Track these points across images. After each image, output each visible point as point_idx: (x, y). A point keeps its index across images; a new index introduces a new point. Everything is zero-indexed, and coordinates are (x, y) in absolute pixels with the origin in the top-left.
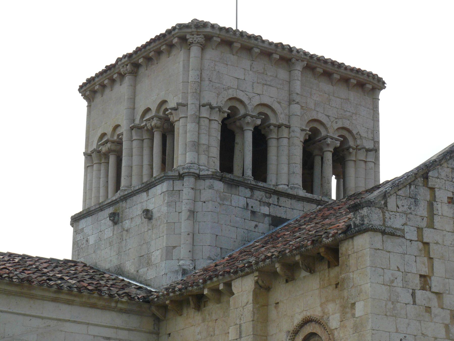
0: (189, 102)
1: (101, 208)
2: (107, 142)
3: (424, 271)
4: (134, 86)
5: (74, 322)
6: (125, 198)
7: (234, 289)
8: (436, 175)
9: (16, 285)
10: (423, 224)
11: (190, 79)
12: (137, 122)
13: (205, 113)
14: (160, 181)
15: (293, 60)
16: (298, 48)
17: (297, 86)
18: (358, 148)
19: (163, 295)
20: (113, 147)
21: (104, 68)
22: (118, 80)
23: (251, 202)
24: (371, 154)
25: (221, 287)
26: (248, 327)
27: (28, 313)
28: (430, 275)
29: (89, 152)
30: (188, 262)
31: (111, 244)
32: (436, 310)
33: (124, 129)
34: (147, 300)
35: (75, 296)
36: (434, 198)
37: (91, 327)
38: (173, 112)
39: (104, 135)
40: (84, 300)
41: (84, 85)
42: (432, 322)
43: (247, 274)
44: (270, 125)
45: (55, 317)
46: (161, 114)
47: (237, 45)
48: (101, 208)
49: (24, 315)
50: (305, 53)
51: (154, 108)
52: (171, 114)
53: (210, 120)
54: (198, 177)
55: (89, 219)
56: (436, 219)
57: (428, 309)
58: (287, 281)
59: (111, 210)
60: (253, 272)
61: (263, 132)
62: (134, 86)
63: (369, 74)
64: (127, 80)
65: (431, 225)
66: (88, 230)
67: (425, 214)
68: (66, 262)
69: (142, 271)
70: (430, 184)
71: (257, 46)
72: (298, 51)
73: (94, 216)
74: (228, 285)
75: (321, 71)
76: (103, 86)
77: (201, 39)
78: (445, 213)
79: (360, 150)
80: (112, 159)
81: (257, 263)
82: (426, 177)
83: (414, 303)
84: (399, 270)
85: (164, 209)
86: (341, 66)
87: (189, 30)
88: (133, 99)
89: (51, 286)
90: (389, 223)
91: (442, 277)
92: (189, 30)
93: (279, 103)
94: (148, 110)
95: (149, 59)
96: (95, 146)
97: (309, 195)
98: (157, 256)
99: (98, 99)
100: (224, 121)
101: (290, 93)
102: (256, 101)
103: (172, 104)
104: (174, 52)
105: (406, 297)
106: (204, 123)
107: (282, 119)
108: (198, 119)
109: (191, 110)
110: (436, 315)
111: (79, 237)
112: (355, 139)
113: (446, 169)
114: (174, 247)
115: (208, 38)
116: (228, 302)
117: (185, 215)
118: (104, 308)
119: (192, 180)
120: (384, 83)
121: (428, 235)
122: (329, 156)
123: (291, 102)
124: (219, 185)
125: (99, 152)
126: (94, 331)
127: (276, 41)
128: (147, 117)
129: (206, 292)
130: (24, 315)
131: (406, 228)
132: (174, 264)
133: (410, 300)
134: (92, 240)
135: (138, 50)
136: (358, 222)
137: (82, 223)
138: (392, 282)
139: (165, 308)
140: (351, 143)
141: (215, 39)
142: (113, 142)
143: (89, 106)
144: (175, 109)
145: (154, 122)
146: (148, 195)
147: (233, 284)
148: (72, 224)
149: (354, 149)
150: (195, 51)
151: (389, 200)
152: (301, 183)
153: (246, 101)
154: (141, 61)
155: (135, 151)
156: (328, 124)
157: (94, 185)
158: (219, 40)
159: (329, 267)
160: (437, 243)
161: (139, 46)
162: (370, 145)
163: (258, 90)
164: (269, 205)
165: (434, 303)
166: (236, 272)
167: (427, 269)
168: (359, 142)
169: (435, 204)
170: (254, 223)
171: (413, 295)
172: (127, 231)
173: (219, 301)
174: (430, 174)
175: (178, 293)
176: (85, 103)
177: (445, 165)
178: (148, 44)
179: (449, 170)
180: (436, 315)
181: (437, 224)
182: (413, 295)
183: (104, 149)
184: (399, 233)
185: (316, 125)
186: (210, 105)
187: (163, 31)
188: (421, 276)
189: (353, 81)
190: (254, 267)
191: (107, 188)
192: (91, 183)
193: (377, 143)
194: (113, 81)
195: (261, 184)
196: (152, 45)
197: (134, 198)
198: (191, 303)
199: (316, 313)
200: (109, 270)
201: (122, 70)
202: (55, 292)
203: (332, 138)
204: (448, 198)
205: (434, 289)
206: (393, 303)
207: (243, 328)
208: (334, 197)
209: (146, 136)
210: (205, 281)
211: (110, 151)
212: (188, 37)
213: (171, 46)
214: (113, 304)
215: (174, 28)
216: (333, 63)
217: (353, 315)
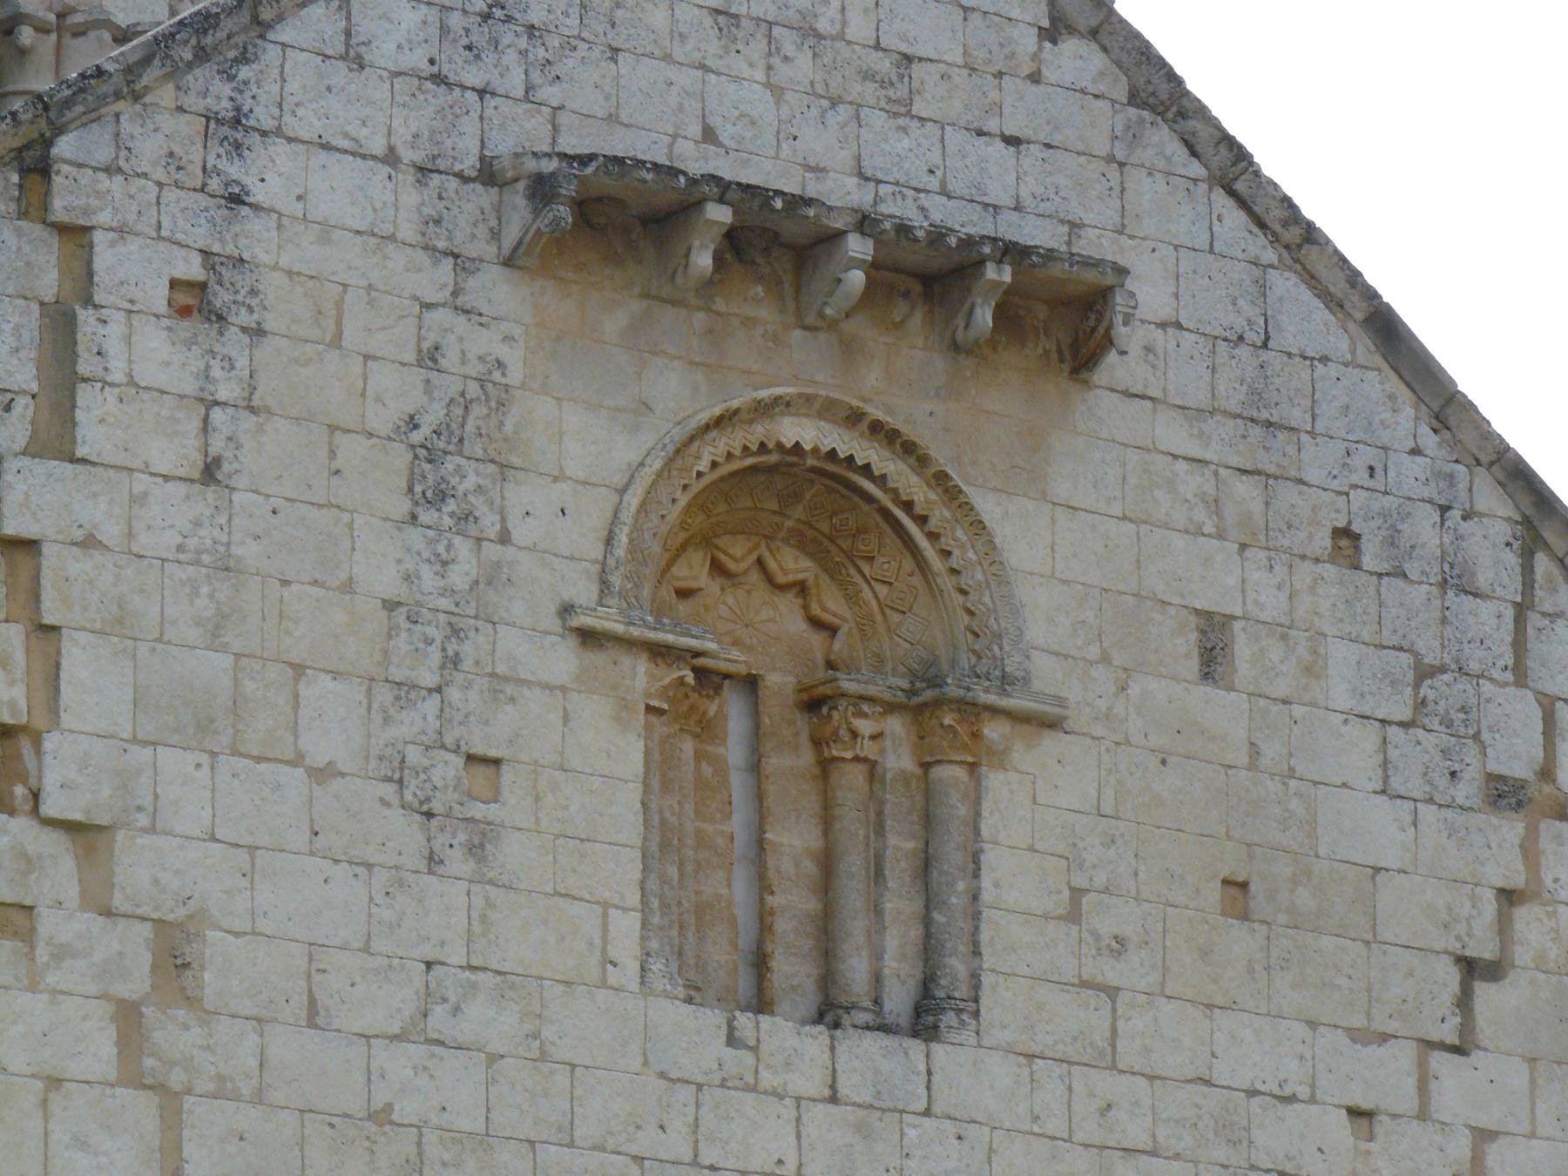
8: (104, 154)
28: (39, 723)
36: (83, 284)
42: (33, 988)
56: (91, 406)
70: (62, 205)
78: (148, 373)
79: (79, 33)
91: (113, 737)
110: (62, 953)
113: (167, 121)
149: (42, 29)
160: (89, 543)
167: (19, 693)
169: (85, 316)
174: (64, 146)
177: (166, 95)
179: (189, 126)
180: (62, 953)
181: (91, 436)
204: (174, 284)
205: (50, 808)
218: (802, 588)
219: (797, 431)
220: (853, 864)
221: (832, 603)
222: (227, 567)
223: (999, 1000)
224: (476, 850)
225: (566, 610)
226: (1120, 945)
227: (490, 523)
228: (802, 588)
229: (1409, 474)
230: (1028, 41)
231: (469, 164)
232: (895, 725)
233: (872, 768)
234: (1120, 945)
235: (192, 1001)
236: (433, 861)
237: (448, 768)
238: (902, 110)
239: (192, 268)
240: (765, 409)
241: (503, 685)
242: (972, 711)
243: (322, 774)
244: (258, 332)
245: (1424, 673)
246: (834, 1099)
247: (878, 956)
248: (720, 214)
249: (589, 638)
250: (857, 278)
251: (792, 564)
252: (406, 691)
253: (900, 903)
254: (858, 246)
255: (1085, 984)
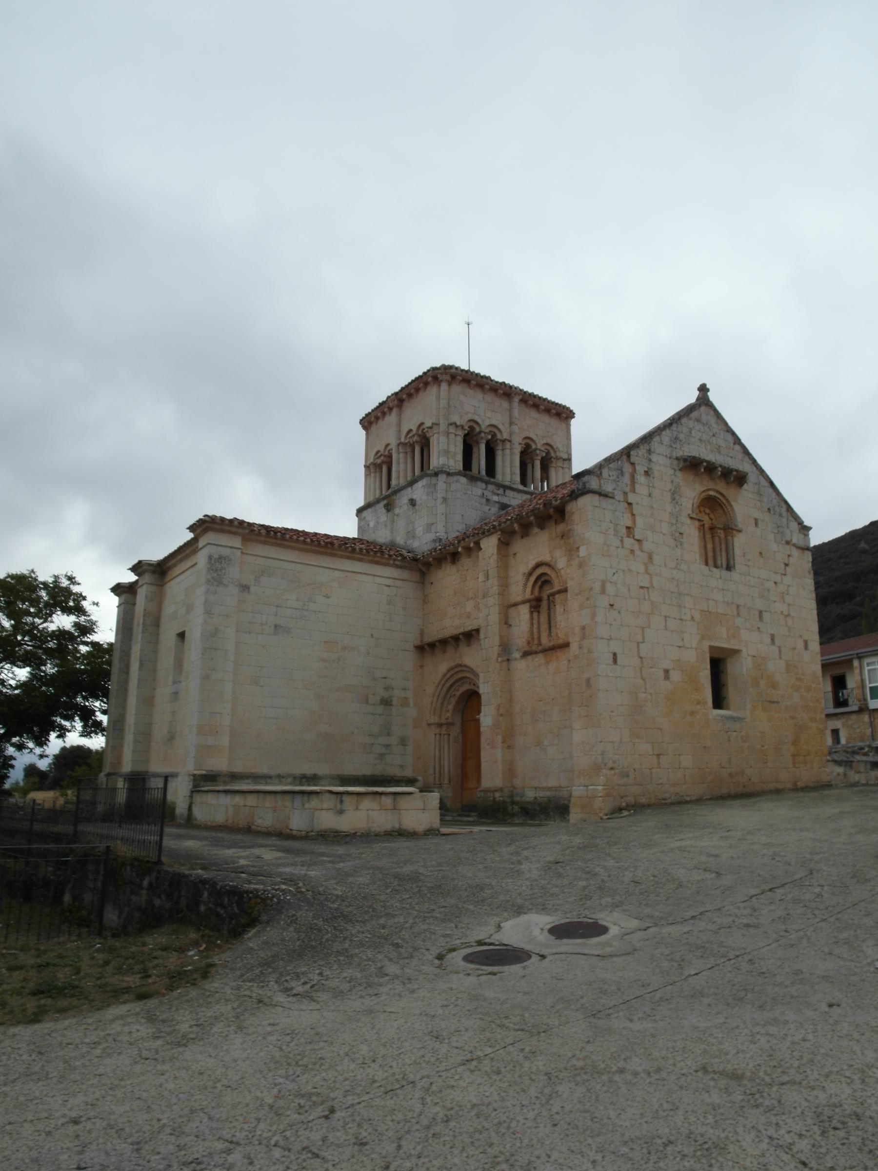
0: (441, 422)
1: (378, 501)
2: (380, 456)
3: (629, 524)
4: (400, 415)
5: (365, 574)
6: (395, 493)
7: (482, 546)
9: (322, 547)
10: (628, 490)
11: (441, 406)
12: (403, 440)
13: (452, 429)
14: (421, 478)
15: (513, 395)
16: (516, 386)
17: (516, 412)
18: (558, 458)
19: (427, 555)
20: (386, 459)
21: (378, 405)
22: (388, 413)
23: (486, 493)
24: (566, 462)
25: (472, 545)
26: (493, 572)
27: (331, 567)
29: (368, 464)
30: (443, 534)
31: (385, 525)
32: (638, 553)
33: (393, 445)
34: (415, 560)
35: (364, 555)
36: (634, 470)
37: (376, 578)
38: (429, 430)
39: (378, 452)
40: (370, 558)
41: (364, 418)
43: (492, 534)
44: (497, 439)
45: (351, 570)
46: (420, 432)
47: (474, 382)
48: (378, 501)
49: (329, 568)
50: (521, 390)
51: (414, 429)
52: (427, 431)
53: (456, 435)
54: (448, 474)
55: (369, 510)
56: (637, 486)
57: (632, 551)
58: (522, 537)
59: (385, 502)
60: (496, 532)
61: (492, 445)
62: (400, 415)
63: (564, 407)
64: (395, 411)
65: (633, 490)
66: (369, 518)
67: (629, 482)
68: (354, 539)
69: (409, 542)
70: (632, 460)
71: (488, 384)
72: (516, 388)
73: (373, 508)
74: (477, 544)
75: (532, 403)
76: (377, 418)
77: (448, 377)
78: (642, 482)
80: (385, 468)
81: (500, 525)
82: (629, 456)
83: (623, 547)
84: (611, 522)
85: (425, 497)
86: (545, 400)
87: (440, 371)
88: (399, 424)
89: (347, 548)
90: (604, 488)
92: (440, 371)
93: (503, 424)
94: (410, 431)
95: (410, 395)
96: (372, 460)
97: (525, 489)
98: (419, 531)
99: (374, 428)
100: (465, 436)
101: (511, 417)
102: (487, 423)
103: (428, 424)
104: (429, 388)
105: (616, 542)
106: (452, 436)
107: (506, 436)
108: (448, 434)
109: (443, 427)
111: (362, 523)
112: (555, 452)
114: (432, 524)
115: (453, 377)
116: (478, 557)
117: (440, 500)
118: (385, 565)
119: (444, 476)
120: (574, 414)
121: (631, 498)
122: (538, 464)
123: (511, 424)
124: (463, 480)
125: (375, 464)
126: (378, 580)
127: (501, 381)
128: (410, 435)
129: (460, 549)
130: (329, 568)
131: (616, 493)
132: (431, 536)
133: (619, 544)
134: (372, 524)
135: (403, 389)
136: (580, 487)
137: (365, 514)
138: (607, 531)
139: (428, 565)
140: (553, 454)
141: (458, 377)
142: (385, 456)
143: (367, 434)
144: (430, 428)
145: (416, 438)
146: (412, 489)
147: (481, 542)
148: (357, 515)
150: (444, 386)
151: (603, 471)
152: (519, 480)
153: (481, 423)
154: (404, 397)
155: (401, 460)
156: (537, 441)
157: (372, 487)
158: (461, 378)
159: (556, 524)
160: (638, 504)
161: (403, 386)
162: (565, 456)
163: (489, 414)
164: (498, 495)
165: (636, 547)
166: (483, 533)
168: (558, 454)
170: (488, 508)
171: (622, 541)
172: (397, 515)
173: (469, 556)
174: (632, 453)
175: (438, 552)
176: (363, 433)
178: (410, 384)
181: (637, 490)
182: (622, 541)
183: (379, 461)
184: (610, 495)
185: (528, 441)
186: (455, 424)
187: (421, 374)
188: (628, 528)
189: (554, 411)
190: (498, 528)
191: (381, 485)
192: (370, 486)
193: (570, 455)
194: (384, 414)
195: (492, 480)
196: (413, 385)
197: (402, 492)
198: (449, 558)
199: (547, 558)
200: (384, 544)
201: (391, 405)
202: (351, 552)
203: (540, 450)
206: (608, 546)
207: (490, 572)
208: (546, 489)
209: (409, 449)
210: (459, 542)
211: (383, 462)
212: (439, 376)
213: (426, 384)
214: (391, 562)
215: (429, 371)
216: (540, 398)
217: (578, 556)
218: (708, 514)
219: (712, 493)
220: (718, 549)
221: (712, 516)
222: (652, 507)
223: (738, 566)
224: (681, 545)
225: (689, 515)
226: (749, 560)
227: (680, 503)
228: (708, 514)
229: (775, 501)
230: (732, 445)
231: (675, 457)
232: (722, 532)
233: (719, 537)
234: (749, 560)
235: (652, 563)
236: (677, 546)
237: (677, 534)
238: (719, 453)
239: (646, 469)
240: (709, 490)
241: (682, 524)
242: (732, 529)
243: (664, 534)
244: (654, 478)
245: (778, 527)
246: (721, 578)
247: (722, 560)
248: (705, 464)
249: (692, 518)
250: (720, 473)
251: (708, 511)
252: (672, 524)
253: (724, 554)
254: (720, 469)
255: (746, 565)
